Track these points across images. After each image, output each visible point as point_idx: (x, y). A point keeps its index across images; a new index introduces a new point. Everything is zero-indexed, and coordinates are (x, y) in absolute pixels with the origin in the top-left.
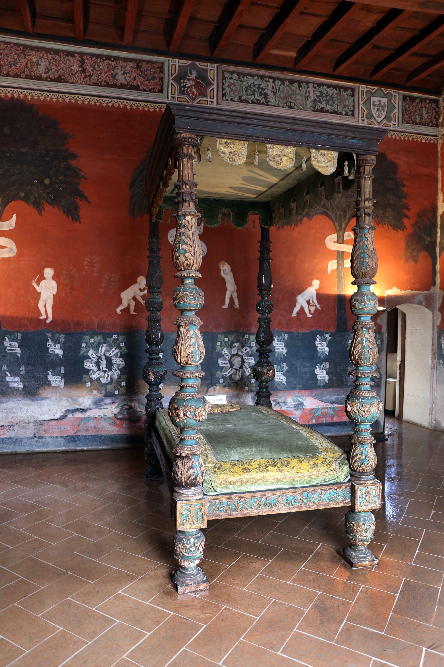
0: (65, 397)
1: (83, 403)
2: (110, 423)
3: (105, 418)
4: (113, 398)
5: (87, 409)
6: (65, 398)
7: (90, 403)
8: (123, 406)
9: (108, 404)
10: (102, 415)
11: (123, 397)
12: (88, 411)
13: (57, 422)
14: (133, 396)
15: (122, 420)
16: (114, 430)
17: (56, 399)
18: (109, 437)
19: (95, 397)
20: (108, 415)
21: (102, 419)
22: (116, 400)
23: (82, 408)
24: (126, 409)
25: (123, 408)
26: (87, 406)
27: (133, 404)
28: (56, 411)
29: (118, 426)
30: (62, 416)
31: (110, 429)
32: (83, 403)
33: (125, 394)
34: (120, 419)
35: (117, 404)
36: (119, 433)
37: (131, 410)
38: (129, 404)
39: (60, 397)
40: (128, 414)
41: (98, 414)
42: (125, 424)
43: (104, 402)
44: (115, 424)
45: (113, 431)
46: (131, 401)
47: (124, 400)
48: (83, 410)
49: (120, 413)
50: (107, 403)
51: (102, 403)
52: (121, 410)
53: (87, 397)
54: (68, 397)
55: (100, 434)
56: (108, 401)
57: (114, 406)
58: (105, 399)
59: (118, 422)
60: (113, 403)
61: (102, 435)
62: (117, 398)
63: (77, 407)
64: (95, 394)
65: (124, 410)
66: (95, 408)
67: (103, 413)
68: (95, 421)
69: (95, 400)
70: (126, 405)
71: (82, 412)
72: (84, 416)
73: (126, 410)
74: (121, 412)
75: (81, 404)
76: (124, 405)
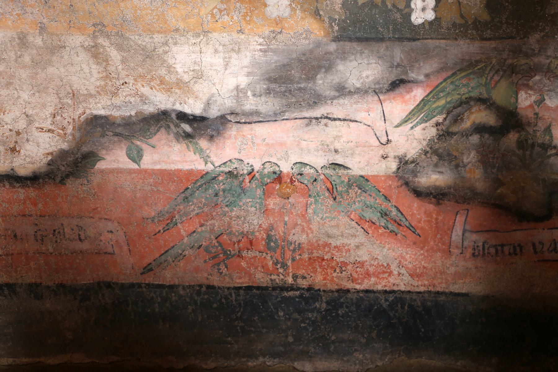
0: (81, 30)
1: (199, 75)
2: (368, 214)
3: (338, 184)
4: (398, 53)
5: (223, 120)
6: (77, 40)
7: (243, 81)
8: (455, 112)
9: (362, 92)
10: (318, 160)
11: (463, 48)
12: (233, 131)
13: (32, 192)
14: (534, 39)
15: (448, 205)
16: (385, 260)
17: (23, 41)
18: (358, 303)
19: (275, 34)
20: (358, 165)
21: (319, 186)
22: (413, 61)
23: (193, 107)
24: (480, 129)
25: (457, 120)
26: (224, 103)
27: (525, 100)
28: (22, 124)
29: (415, 235)
30: (63, 154)
31: (363, 255)
32: (199, 75)
33: (478, 25)
34: (436, 196)
35: (419, 94)
36: (420, 285)
37: (513, 137)
38: (500, 94)
39: (43, 29)
40: (486, 159)
41: (295, 159)
42: (461, 227)
43: (334, 78)
44: (394, 226)
45: (386, 271)
46: (519, 73)
47: (468, 67)
48: (197, 127)
49: (439, 152)
50: (354, 82)
51: (323, 83)
52: (445, 134)
53: (225, 38)
54: (100, 28)
55: (304, 284)
56: (363, 68)
57: (398, 107)
58: (344, 56)
59: (417, 211)
60: (397, 85)
61: (313, 294)
62: (426, 54)
63: (161, 101)
64: (279, 21)
65: (466, 134)
66: (275, 117)
67: (325, 148)
68: (273, 203)
69: (274, 58)
70: (481, 101)
71: (188, 136)
72: (200, 166)
73: (475, 139)
74: (441, 146)
75: (180, 84)
76: (465, 103)
